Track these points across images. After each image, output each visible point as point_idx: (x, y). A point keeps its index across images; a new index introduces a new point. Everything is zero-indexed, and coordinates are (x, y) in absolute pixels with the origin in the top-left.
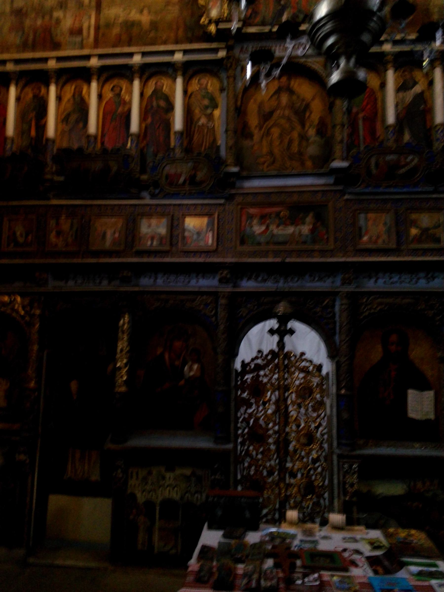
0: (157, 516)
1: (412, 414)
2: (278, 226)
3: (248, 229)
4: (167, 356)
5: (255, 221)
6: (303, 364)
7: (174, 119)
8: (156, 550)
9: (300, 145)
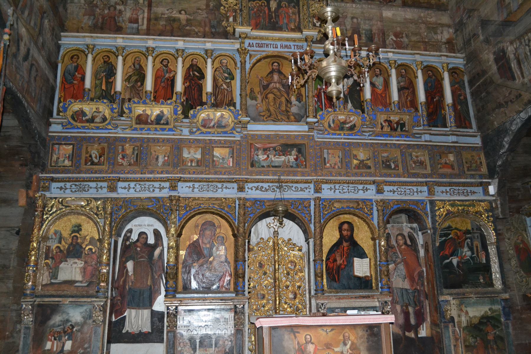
2: (275, 156)
3: (256, 157)
4: (200, 241)
5: (260, 152)
7: (206, 85)
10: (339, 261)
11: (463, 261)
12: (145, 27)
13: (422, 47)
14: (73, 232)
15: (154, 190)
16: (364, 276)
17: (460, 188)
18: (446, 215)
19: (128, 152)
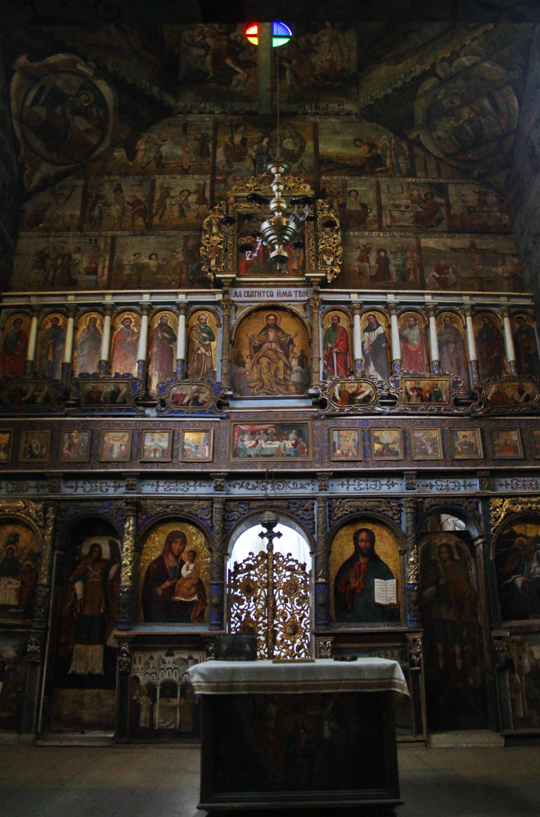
0: (158, 696)
1: (378, 600)
2: (266, 441)
3: (240, 443)
5: (246, 437)
6: (291, 563)
7: (176, 349)
8: (157, 728)
9: (285, 373)
10: (354, 584)
11: (530, 580)
12: (105, 278)
13: (476, 284)
14: (9, 543)
15: (107, 490)
16: (388, 603)
17: (526, 479)
18: (505, 516)
19: (76, 441)
